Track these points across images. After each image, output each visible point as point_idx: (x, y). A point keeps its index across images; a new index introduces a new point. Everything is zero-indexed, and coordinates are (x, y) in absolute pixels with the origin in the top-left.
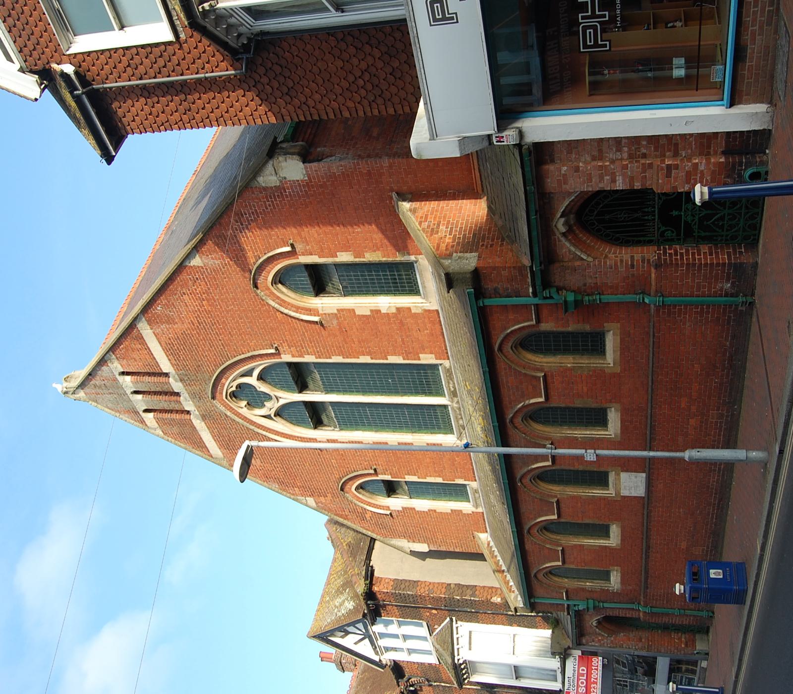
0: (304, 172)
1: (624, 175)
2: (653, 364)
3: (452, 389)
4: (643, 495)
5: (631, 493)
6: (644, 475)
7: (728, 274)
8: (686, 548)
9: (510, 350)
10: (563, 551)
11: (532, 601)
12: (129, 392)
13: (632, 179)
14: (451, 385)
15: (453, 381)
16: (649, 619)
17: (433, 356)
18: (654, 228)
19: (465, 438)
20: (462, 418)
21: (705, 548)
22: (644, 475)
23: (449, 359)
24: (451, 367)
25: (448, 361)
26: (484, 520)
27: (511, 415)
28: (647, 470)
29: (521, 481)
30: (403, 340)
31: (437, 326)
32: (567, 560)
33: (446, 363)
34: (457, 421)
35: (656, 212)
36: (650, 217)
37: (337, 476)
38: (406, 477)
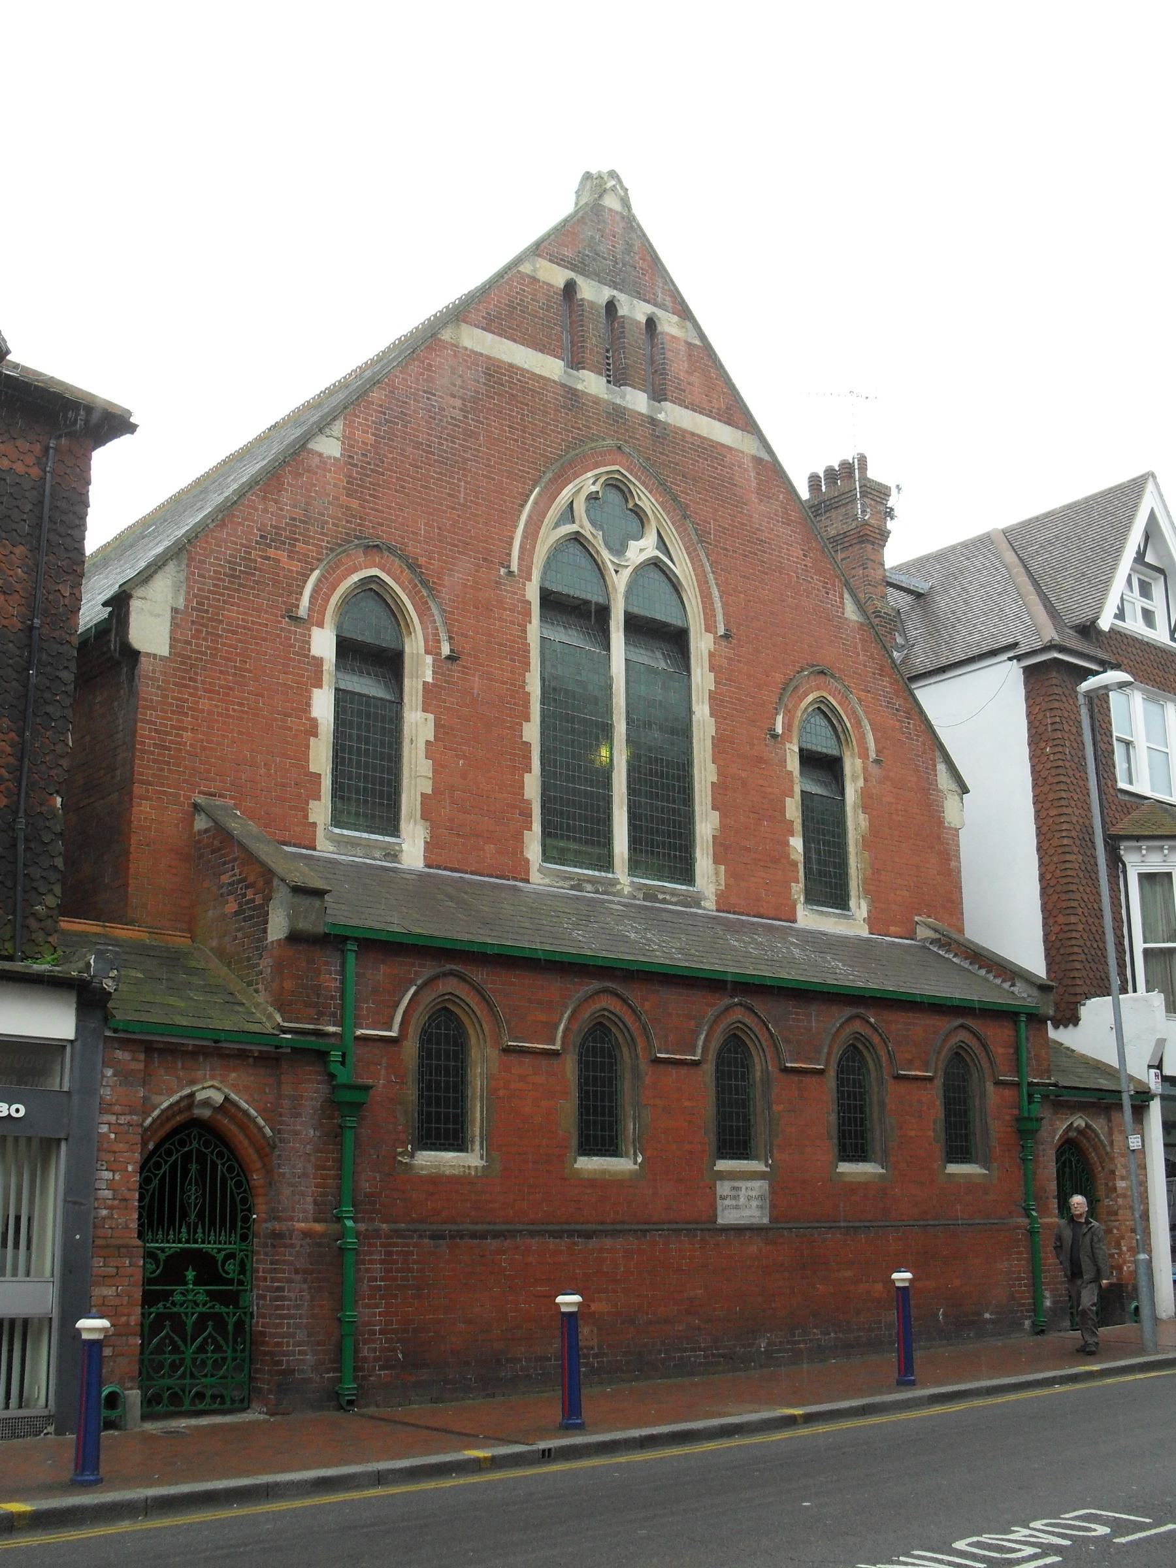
0: (952, 825)
1: (1126, 1188)
2: (816, 1228)
3: (661, 897)
4: (720, 1221)
5: (723, 1198)
6: (766, 1220)
7: (1059, 1301)
8: (594, 1312)
9: (958, 1039)
10: (555, 1054)
11: (352, 946)
12: (581, 281)
13: (1124, 1196)
14: (668, 897)
15: (675, 904)
16: (292, 1246)
17: (723, 887)
18: (225, 1243)
19: (541, 882)
20: (597, 892)
21: (596, 1351)
22: (766, 1220)
23: (718, 911)
24: (705, 909)
25: (715, 909)
26: (438, 867)
27: (872, 1020)
28: (775, 1225)
29: (740, 1004)
30: (748, 850)
31: (772, 913)
32: (513, 1058)
33: (710, 904)
34: (589, 882)
35: (196, 1246)
36: (184, 1235)
37: (422, 560)
38: (431, 717)
